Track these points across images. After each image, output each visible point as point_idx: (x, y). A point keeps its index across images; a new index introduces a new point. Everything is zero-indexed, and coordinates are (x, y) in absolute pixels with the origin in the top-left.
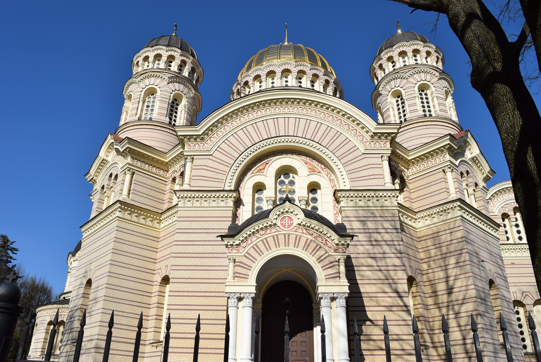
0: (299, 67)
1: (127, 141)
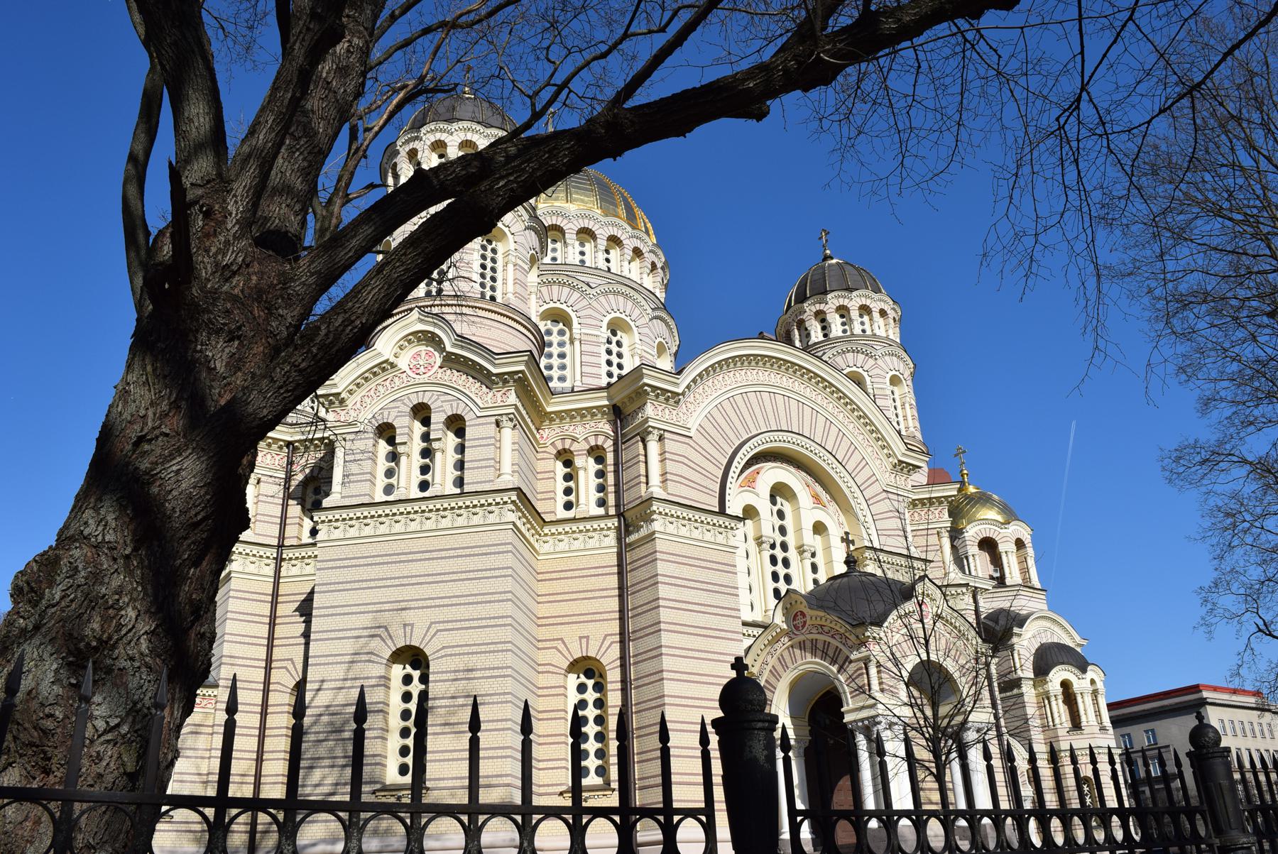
0: (586, 221)
1: (526, 358)
